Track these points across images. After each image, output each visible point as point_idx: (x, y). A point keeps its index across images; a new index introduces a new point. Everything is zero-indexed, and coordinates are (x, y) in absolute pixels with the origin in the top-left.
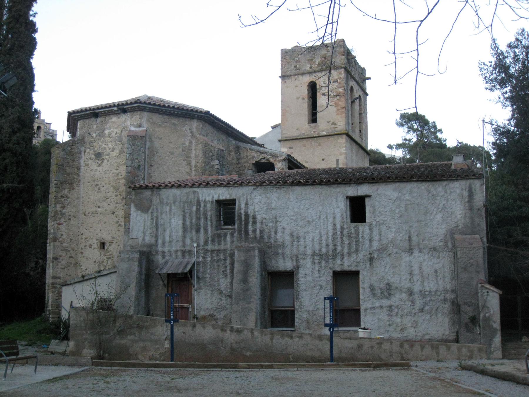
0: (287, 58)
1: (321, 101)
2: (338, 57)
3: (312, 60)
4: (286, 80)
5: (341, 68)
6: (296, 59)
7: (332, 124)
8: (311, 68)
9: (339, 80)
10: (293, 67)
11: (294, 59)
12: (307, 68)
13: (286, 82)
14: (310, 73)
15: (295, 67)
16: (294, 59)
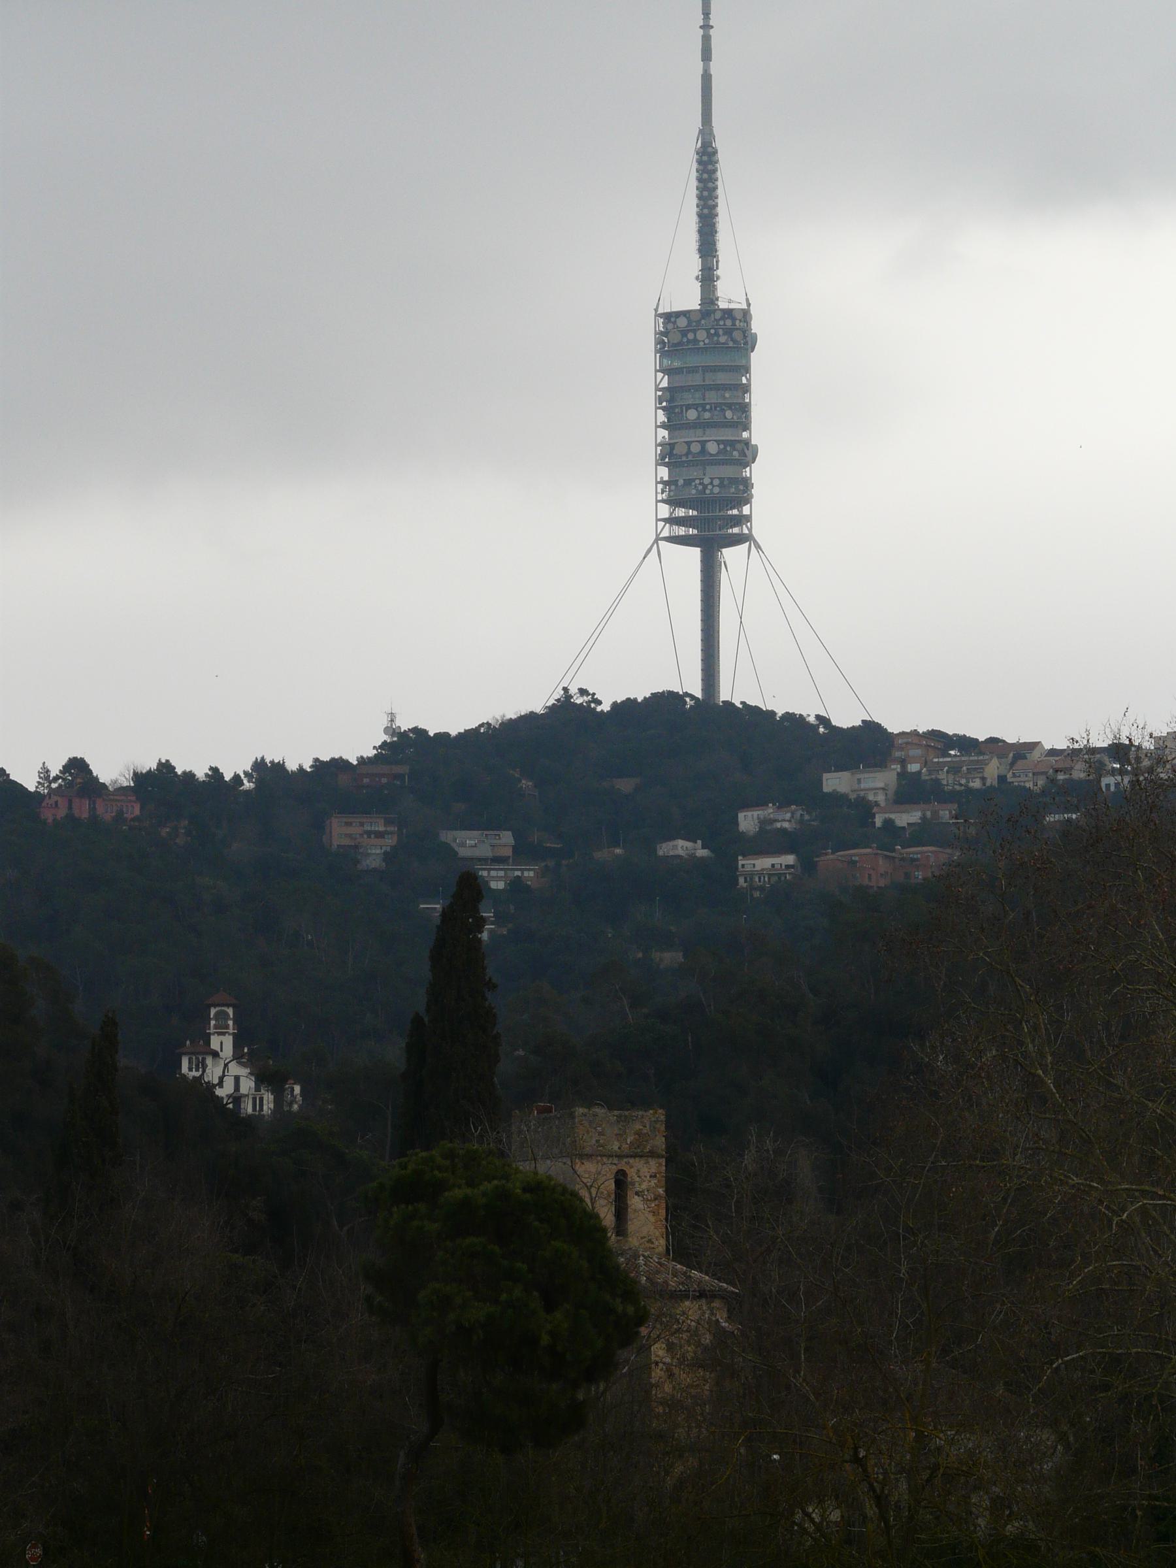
0: (585, 1125)
1: (635, 1202)
2: (657, 1138)
3: (621, 1135)
4: (584, 1162)
5: (663, 1157)
6: (598, 1128)
7: (648, 1242)
8: (619, 1148)
9: (658, 1175)
10: (594, 1142)
11: (595, 1128)
12: (614, 1147)
13: (583, 1164)
14: (620, 1157)
15: (597, 1141)
16: (595, 1128)
